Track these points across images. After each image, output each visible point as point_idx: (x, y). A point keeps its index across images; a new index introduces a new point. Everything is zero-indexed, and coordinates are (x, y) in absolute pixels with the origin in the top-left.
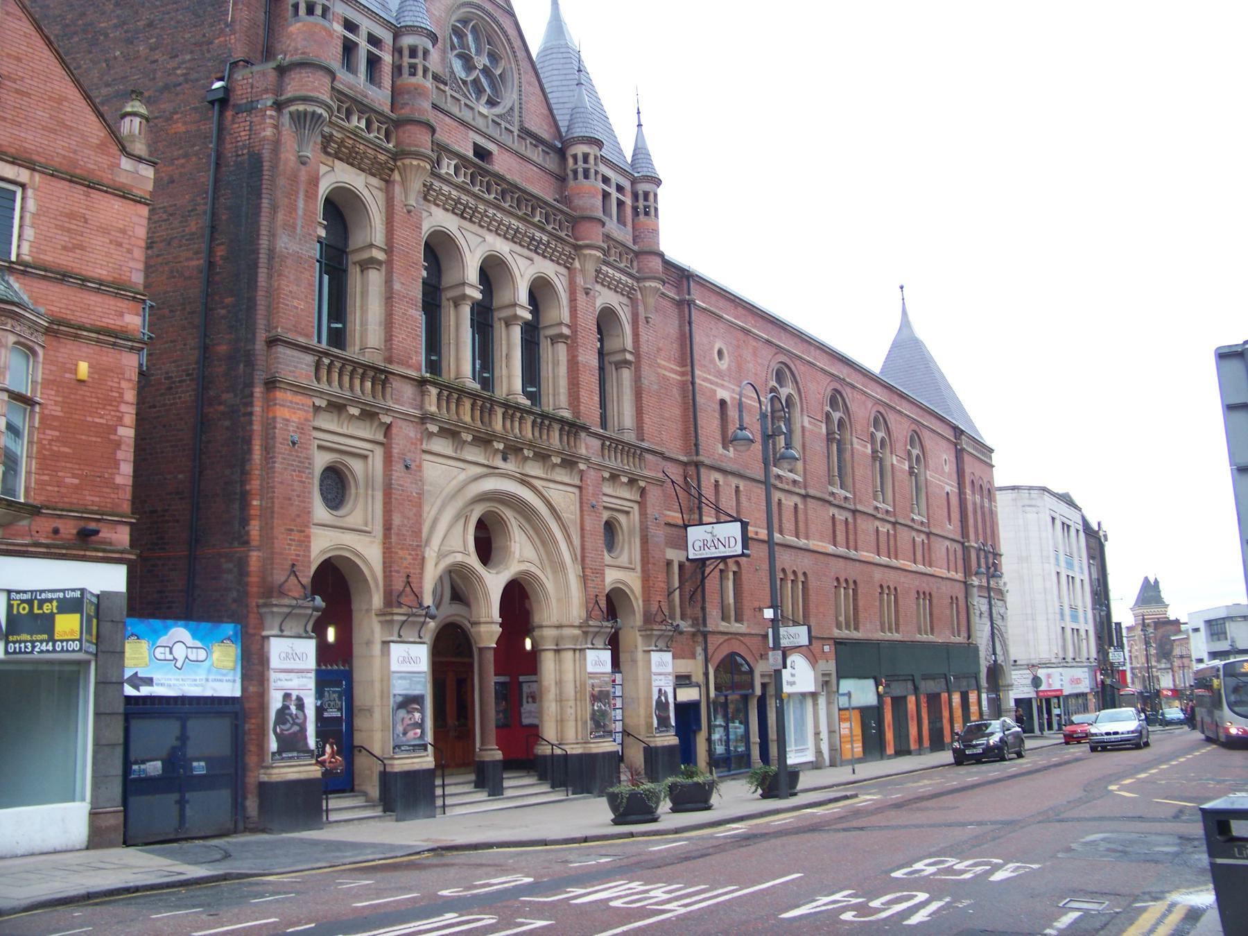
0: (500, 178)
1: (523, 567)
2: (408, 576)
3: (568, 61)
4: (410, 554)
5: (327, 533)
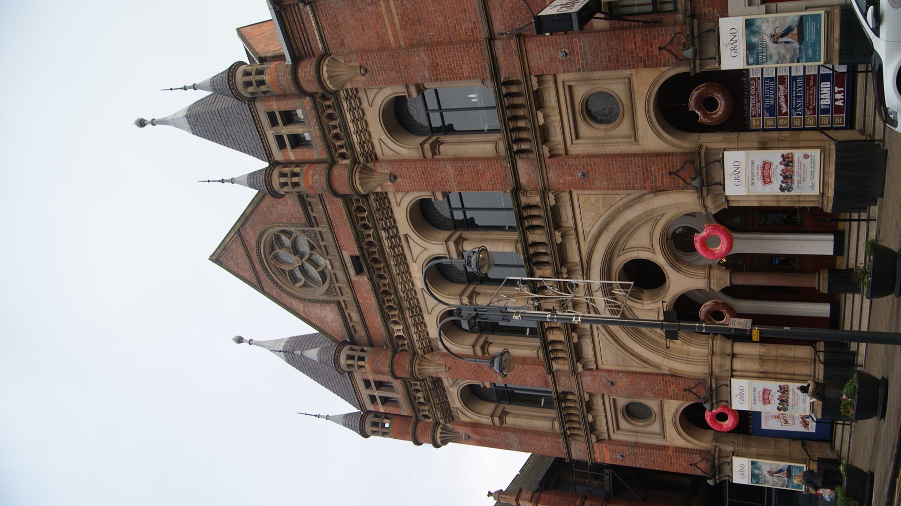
0: (359, 239)
1: (657, 247)
2: (685, 390)
3: (198, 116)
4: (670, 387)
5: (667, 431)
